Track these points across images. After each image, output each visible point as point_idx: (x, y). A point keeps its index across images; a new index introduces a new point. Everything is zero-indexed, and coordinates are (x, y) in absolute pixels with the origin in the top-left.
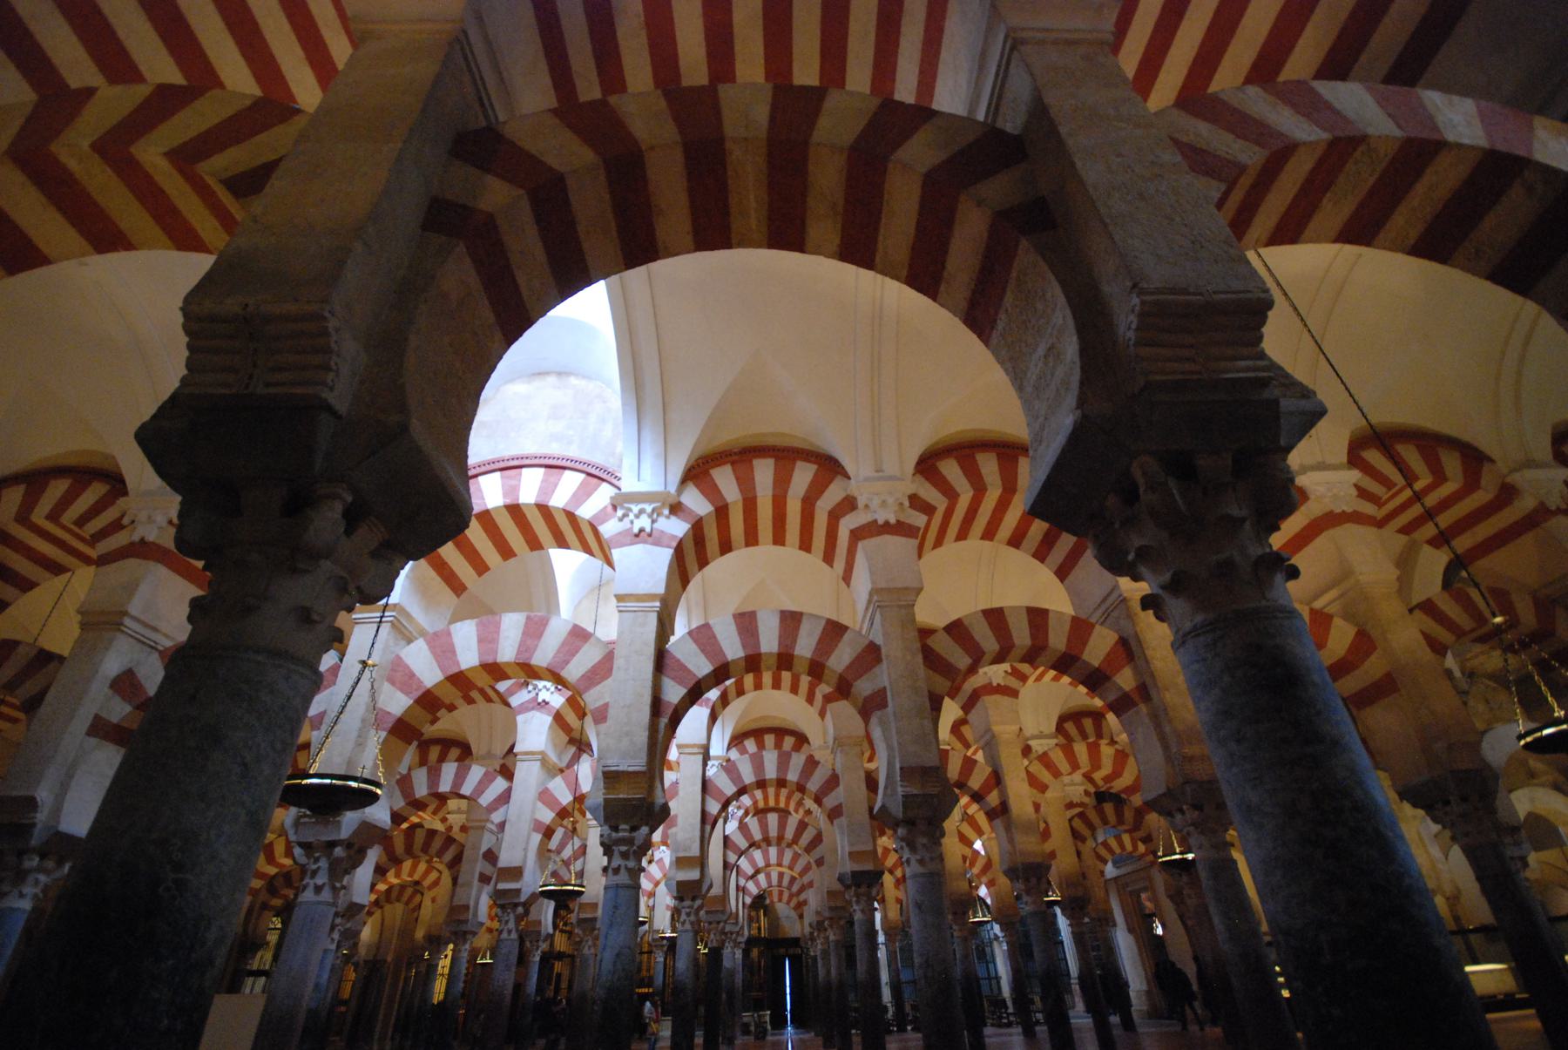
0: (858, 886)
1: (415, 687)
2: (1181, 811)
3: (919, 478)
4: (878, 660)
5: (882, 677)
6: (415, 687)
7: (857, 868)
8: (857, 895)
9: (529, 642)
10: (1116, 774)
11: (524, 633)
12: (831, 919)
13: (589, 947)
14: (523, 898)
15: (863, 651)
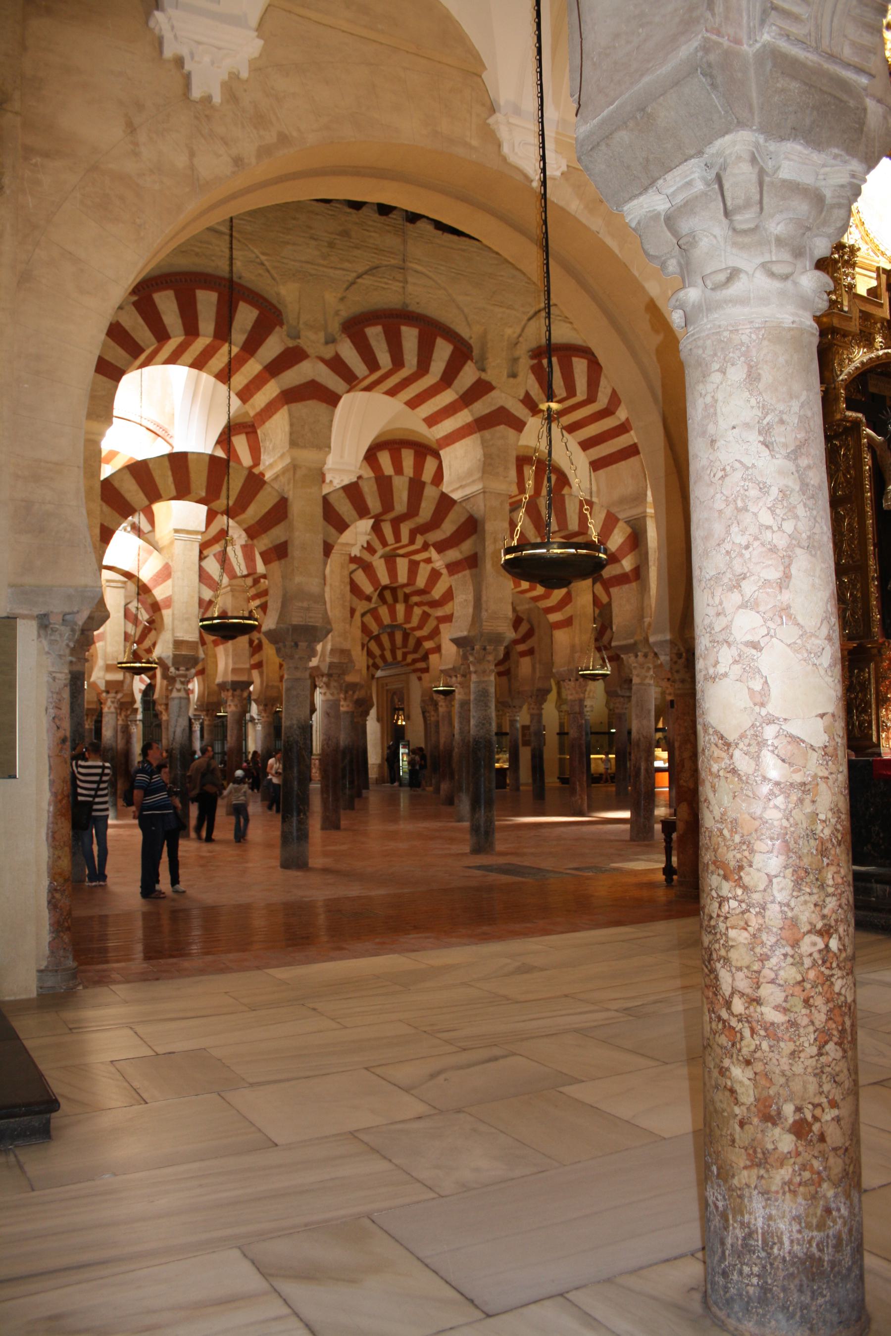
0: (234, 690)
2: (456, 676)
3: (365, 464)
8: (233, 696)
10: (420, 627)
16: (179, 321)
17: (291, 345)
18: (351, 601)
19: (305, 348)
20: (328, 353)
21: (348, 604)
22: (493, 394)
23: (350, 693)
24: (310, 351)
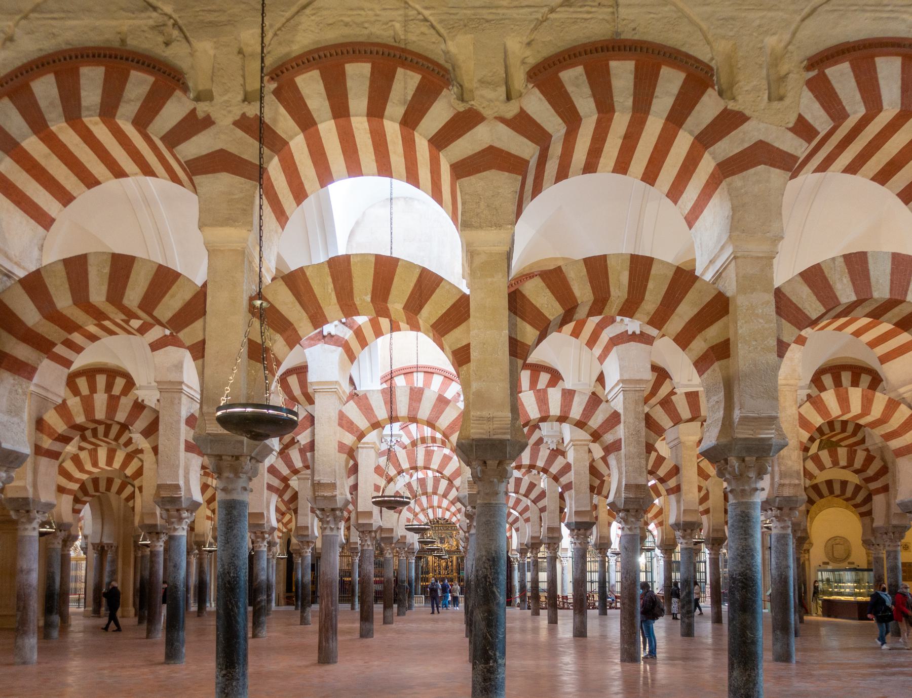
1: (355, 430)
4: (619, 422)
5: (620, 432)
6: (355, 430)
7: (579, 520)
9: (414, 404)
11: (410, 399)
12: (549, 544)
13: (390, 554)
14: (374, 529)
15: (610, 416)
16: (327, 104)
17: (462, 109)
18: (647, 436)
19: (481, 109)
20: (511, 110)
21: (643, 440)
22: (746, 126)
23: (689, 531)
24: (486, 112)
